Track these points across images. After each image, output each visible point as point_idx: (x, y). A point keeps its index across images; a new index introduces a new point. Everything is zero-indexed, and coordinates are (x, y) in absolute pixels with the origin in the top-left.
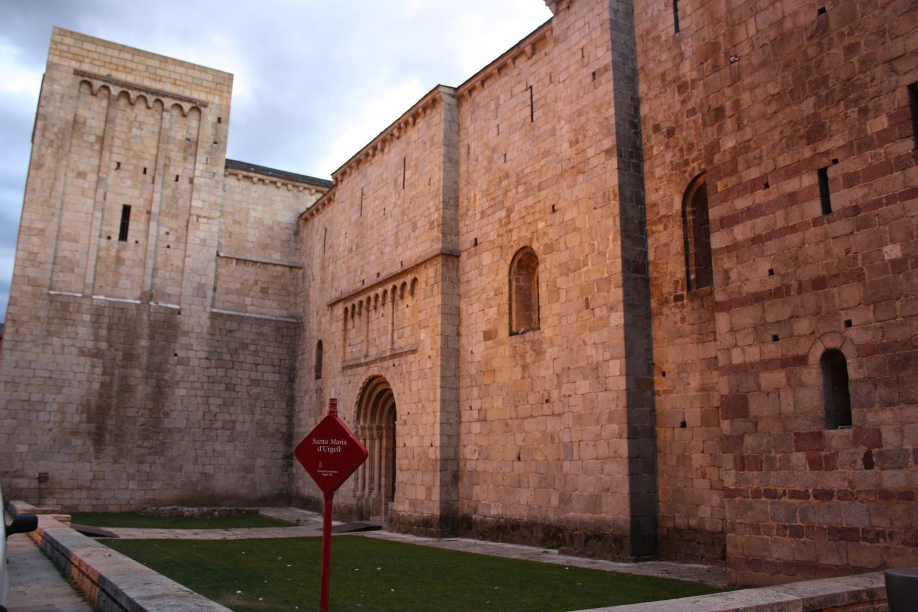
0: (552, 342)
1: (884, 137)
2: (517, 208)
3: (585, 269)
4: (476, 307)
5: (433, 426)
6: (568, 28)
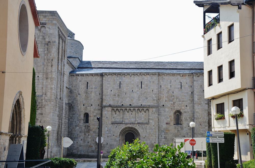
0: (185, 127)
4: (163, 118)
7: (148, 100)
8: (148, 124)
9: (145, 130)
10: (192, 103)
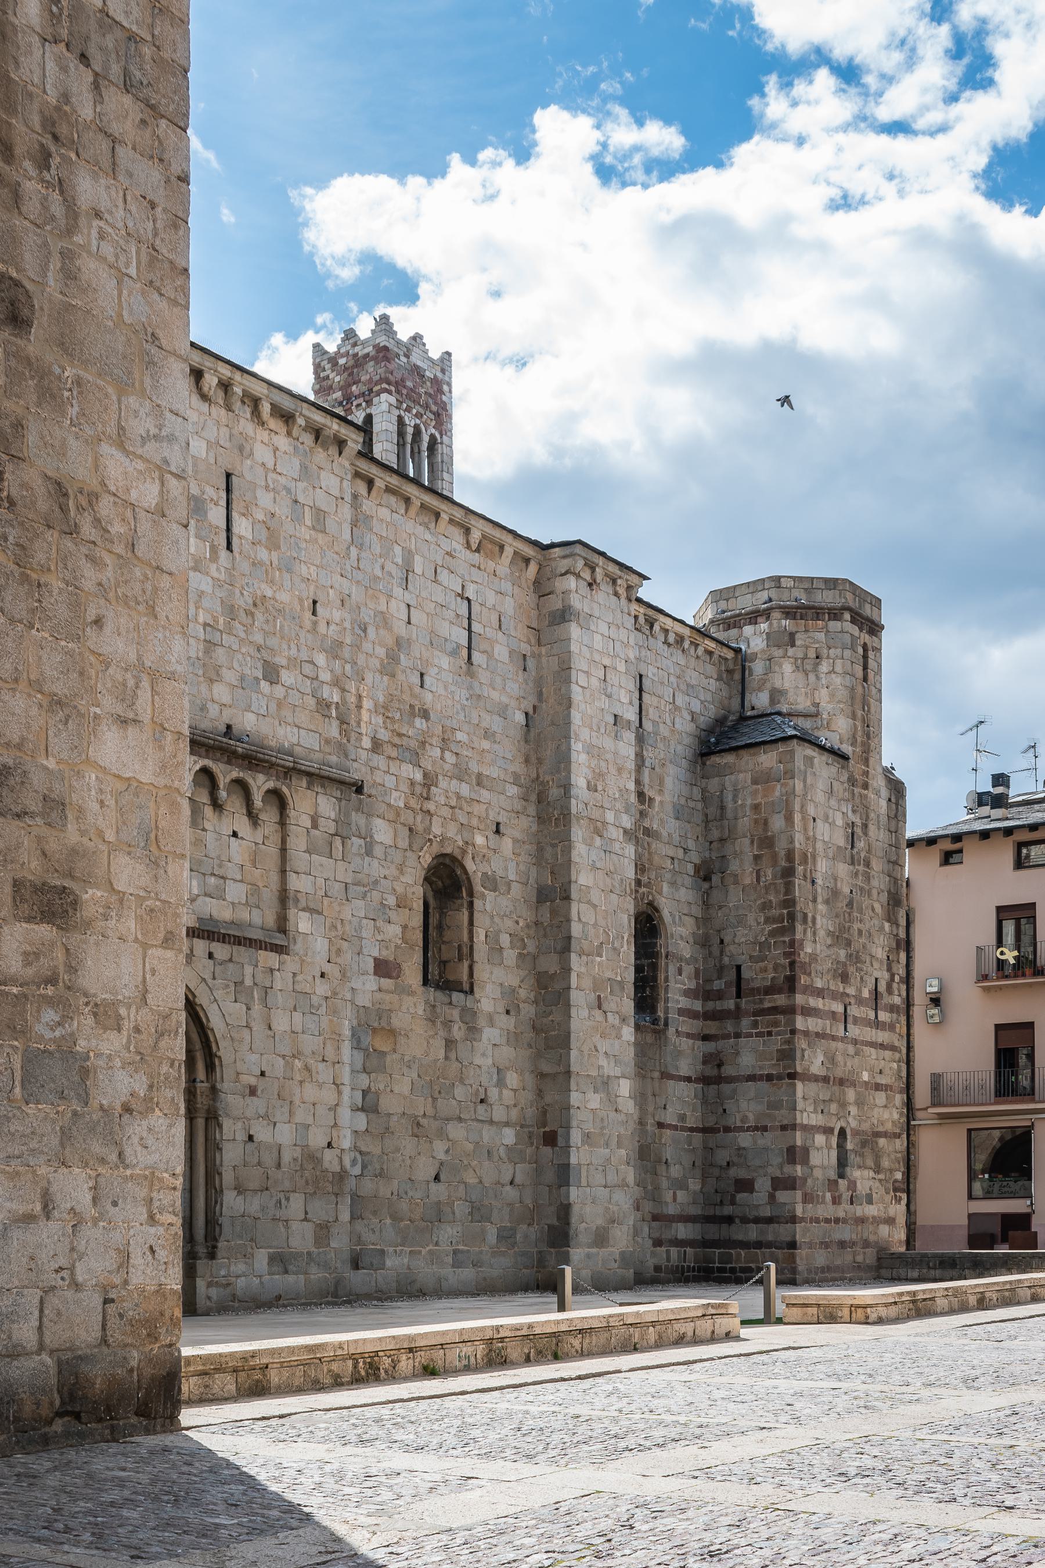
2: (443, 783)
5: (334, 1108)
8: (280, 949)
9: (257, 1007)
10: (532, 810)
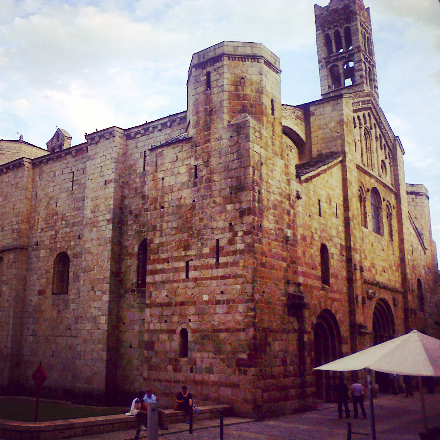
1: (208, 256)
2: (61, 231)
3: (93, 272)
4: (35, 277)
6: (95, 154)
7: (4, 232)
